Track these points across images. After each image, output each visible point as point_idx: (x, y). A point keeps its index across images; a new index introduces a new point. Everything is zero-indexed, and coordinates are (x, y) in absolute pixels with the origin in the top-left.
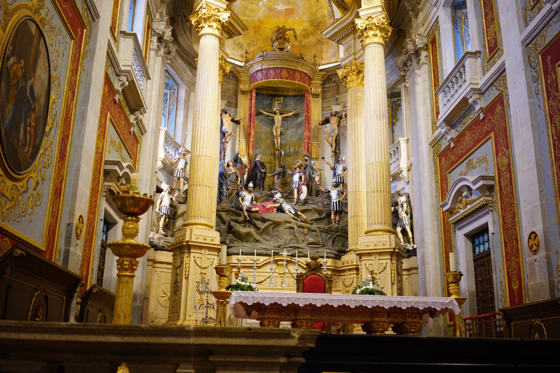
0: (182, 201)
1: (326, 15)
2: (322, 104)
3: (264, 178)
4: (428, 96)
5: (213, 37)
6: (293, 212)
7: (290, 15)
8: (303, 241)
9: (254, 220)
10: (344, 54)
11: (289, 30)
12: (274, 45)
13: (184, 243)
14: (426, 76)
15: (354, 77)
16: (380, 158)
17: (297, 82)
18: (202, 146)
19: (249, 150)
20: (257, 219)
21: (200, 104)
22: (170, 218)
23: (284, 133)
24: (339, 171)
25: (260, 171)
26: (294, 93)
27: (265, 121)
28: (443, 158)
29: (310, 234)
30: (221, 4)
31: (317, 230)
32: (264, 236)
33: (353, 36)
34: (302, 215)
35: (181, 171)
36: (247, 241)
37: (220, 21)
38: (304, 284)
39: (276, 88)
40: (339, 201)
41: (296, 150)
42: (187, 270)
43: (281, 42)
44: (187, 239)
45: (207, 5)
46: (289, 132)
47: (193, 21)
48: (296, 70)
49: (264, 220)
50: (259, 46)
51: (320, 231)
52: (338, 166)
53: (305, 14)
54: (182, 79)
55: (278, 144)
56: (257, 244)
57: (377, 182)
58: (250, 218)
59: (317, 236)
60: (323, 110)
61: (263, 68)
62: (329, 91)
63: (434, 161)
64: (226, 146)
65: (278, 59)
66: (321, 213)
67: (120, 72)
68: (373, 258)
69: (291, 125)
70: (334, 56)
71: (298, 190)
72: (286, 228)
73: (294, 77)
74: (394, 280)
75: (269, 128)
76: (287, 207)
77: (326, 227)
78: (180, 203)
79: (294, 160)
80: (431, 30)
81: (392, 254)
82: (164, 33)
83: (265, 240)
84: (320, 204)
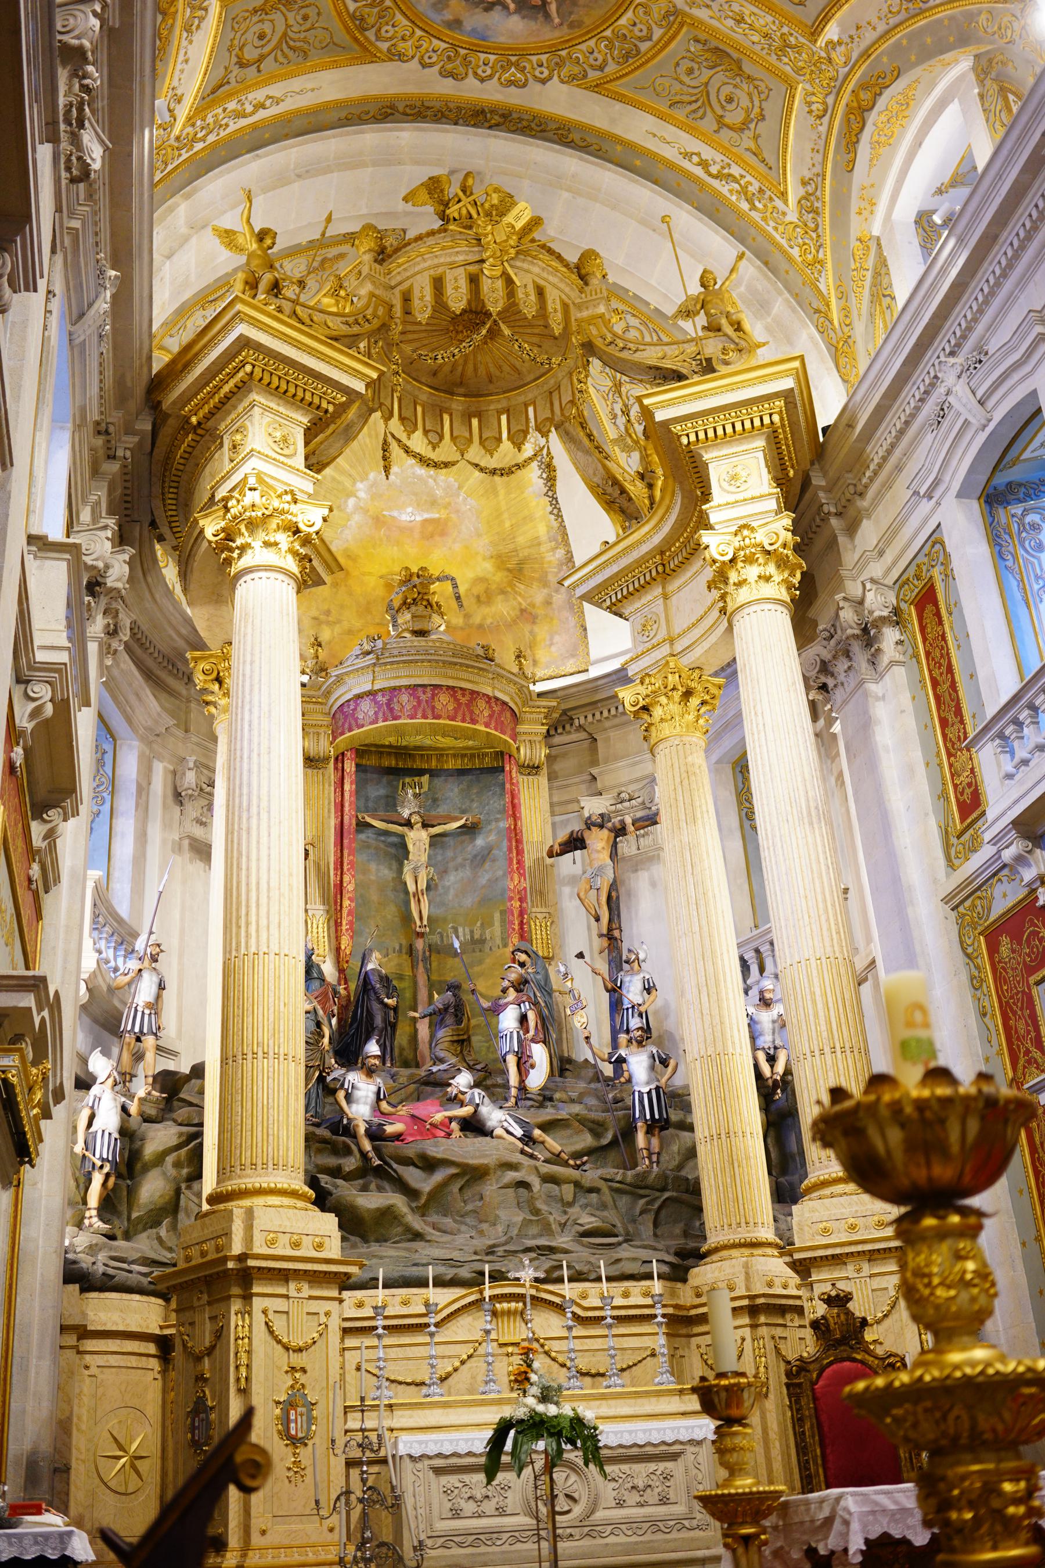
0: (152, 1112)
1: (544, 538)
2: (551, 796)
3: (394, 1026)
4: (917, 756)
5: (281, 577)
6: (519, 1132)
7: (437, 538)
9: (395, 1166)
10: (634, 640)
11: (438, 579)
12: (400, 621)
13: (230, 1265)
14: (905, 699)
15: (675, 708)
16: (827, 944)
17: (482, 728)
18: (263, 922)
19: (338, 939)
20: (407, 1162)
21: (249, 785)
22: (119, 1176)
23: (436, 885)
24: (633, 992)
25: (382, 1002)
26: (459, 762)
27: (376, 848)
28: (1005, 940)
29: (583, 1201)
30: (299, 479)
31: (602, 1185)
32: (434, 1218)
33: (660, 590)
34: (549, 1140)
35: (147, 1012)
36: (382, 1240)
37: (297, 531)
38: (815, 1399)
39: (405, 747)
40: (657, 1088)
41: (477, 936)
42: (244, 1360)
43: (419, 613)
44: (237, 1248)
45: (260, 480)
46: (452, 879)
47: (211, 527)
48: (478, 693)
49: (429, 1164)
50: (346, 625)
51: (611, 1189)
52: (627, 979)
53: (479, 536)
54: (129, 720)
55: (421, 919)
56: (418, 1245)
57: (829, 1023)
58: (380, 1159)
59: (604, 1206)
60: (553, 814)
61: (376, 687)
62: (564, 755)
63: (964, 950)
65: (423, 661)
66: (600, 1130)
67: (31, 668)
68: (850, 1270)
69: (454, 859)
70: (573, 656)
71: (519, 1059)
72: (506, 1187)
73: (472, 712)
75: (391, 869)
76: (494, 1116)
77: (630, 1173)
78: (147, 1119)
80: (913, 567)
82: (107, 567)
83: (439, 1230)
84: (592, 1101)
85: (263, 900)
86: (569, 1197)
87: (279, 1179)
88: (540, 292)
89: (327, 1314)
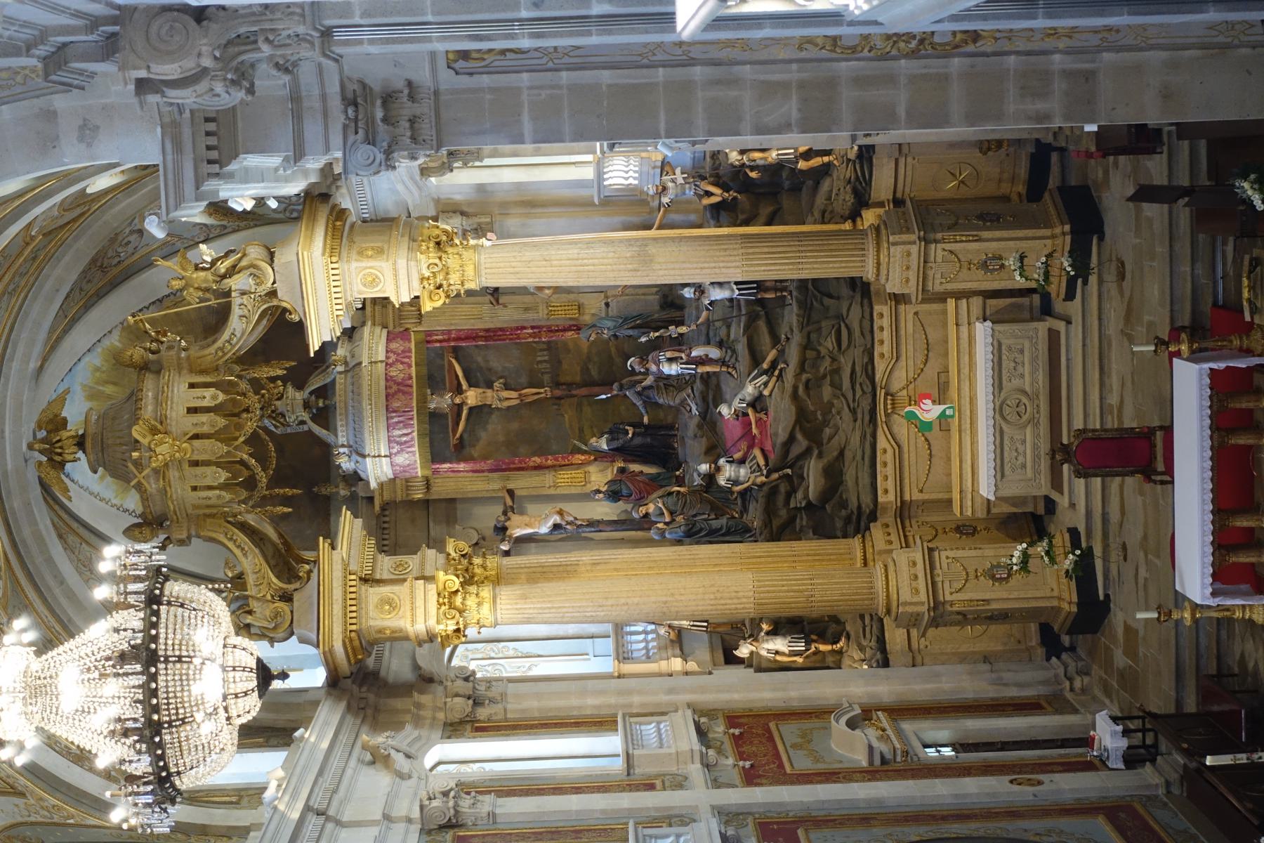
6: (764, 378)
8: (834, 360)
25: (632, 438)
36: (841, 473)
46: (496, 363)
49: (791, 439)
51: (808, 324)
56: (848, 455)
59: (819, 329)
64: (583, 520)
72: (809, 396)
74: (973, 236)
76: (750, 390)
79: (568, 351)
81: (927, 242)
85: (723, 602)
86: (814, 353)
87: (880, 586)
88: (192, 411)
89: (947, 558)
